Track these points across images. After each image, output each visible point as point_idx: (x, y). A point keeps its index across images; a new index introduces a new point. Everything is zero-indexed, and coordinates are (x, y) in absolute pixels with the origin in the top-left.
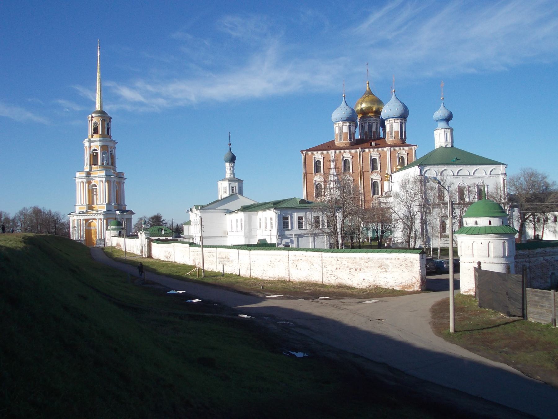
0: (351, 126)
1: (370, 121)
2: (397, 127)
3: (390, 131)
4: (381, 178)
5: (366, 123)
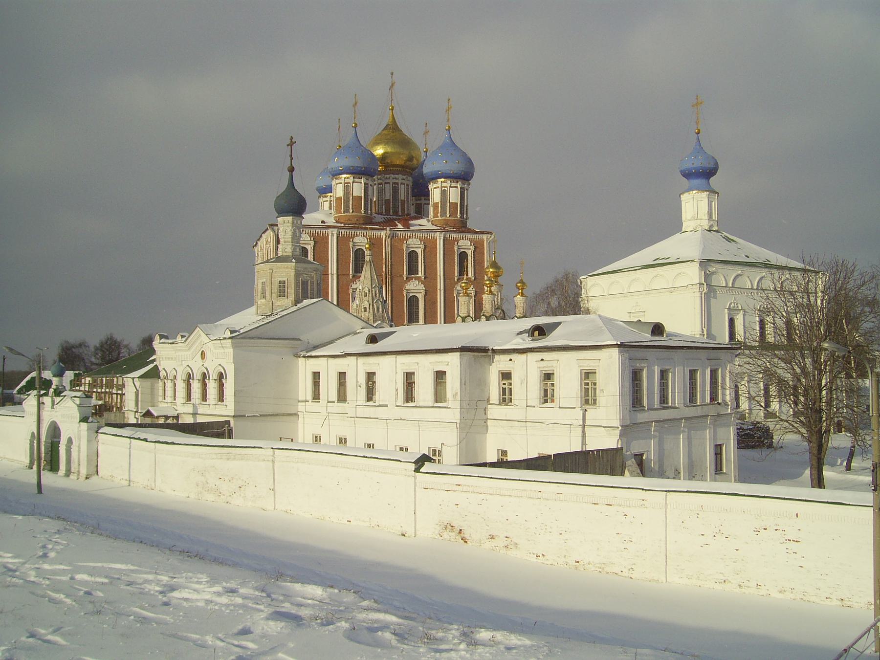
0: (367, 184)
1: (397, 181)
2: (454, 196)
3: (441, 201)
4: (425, 290)
5: (389, 183)
